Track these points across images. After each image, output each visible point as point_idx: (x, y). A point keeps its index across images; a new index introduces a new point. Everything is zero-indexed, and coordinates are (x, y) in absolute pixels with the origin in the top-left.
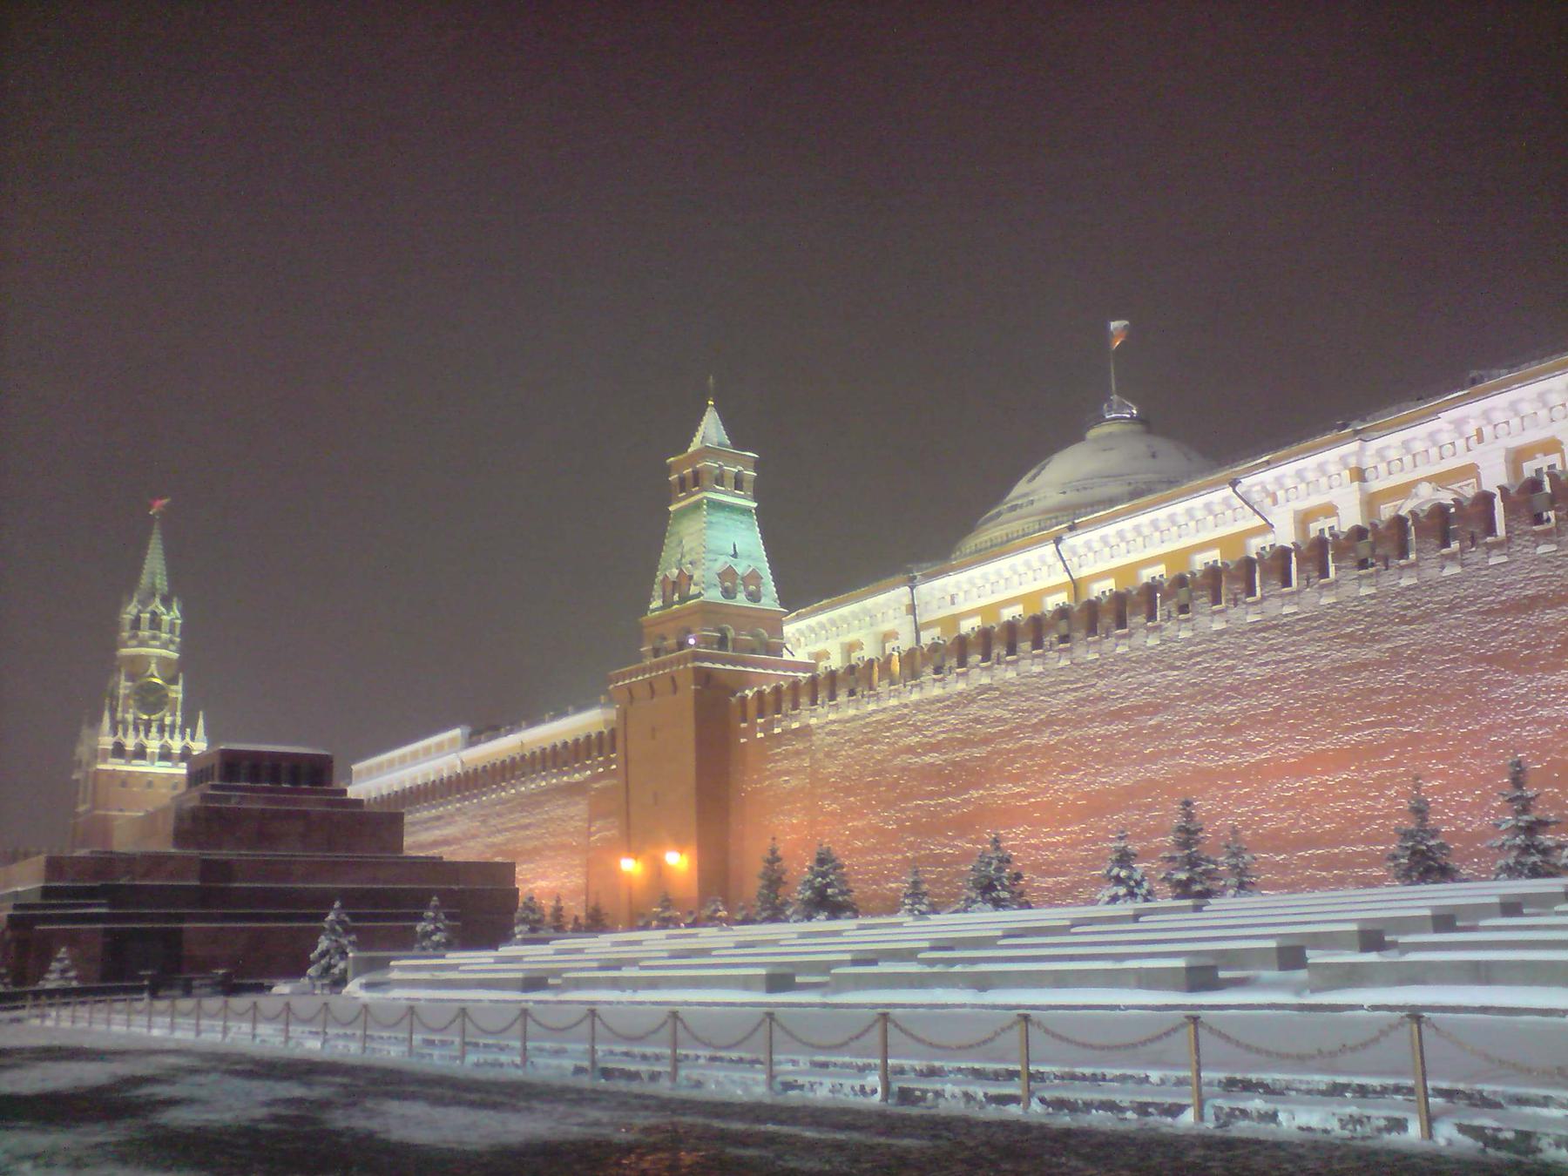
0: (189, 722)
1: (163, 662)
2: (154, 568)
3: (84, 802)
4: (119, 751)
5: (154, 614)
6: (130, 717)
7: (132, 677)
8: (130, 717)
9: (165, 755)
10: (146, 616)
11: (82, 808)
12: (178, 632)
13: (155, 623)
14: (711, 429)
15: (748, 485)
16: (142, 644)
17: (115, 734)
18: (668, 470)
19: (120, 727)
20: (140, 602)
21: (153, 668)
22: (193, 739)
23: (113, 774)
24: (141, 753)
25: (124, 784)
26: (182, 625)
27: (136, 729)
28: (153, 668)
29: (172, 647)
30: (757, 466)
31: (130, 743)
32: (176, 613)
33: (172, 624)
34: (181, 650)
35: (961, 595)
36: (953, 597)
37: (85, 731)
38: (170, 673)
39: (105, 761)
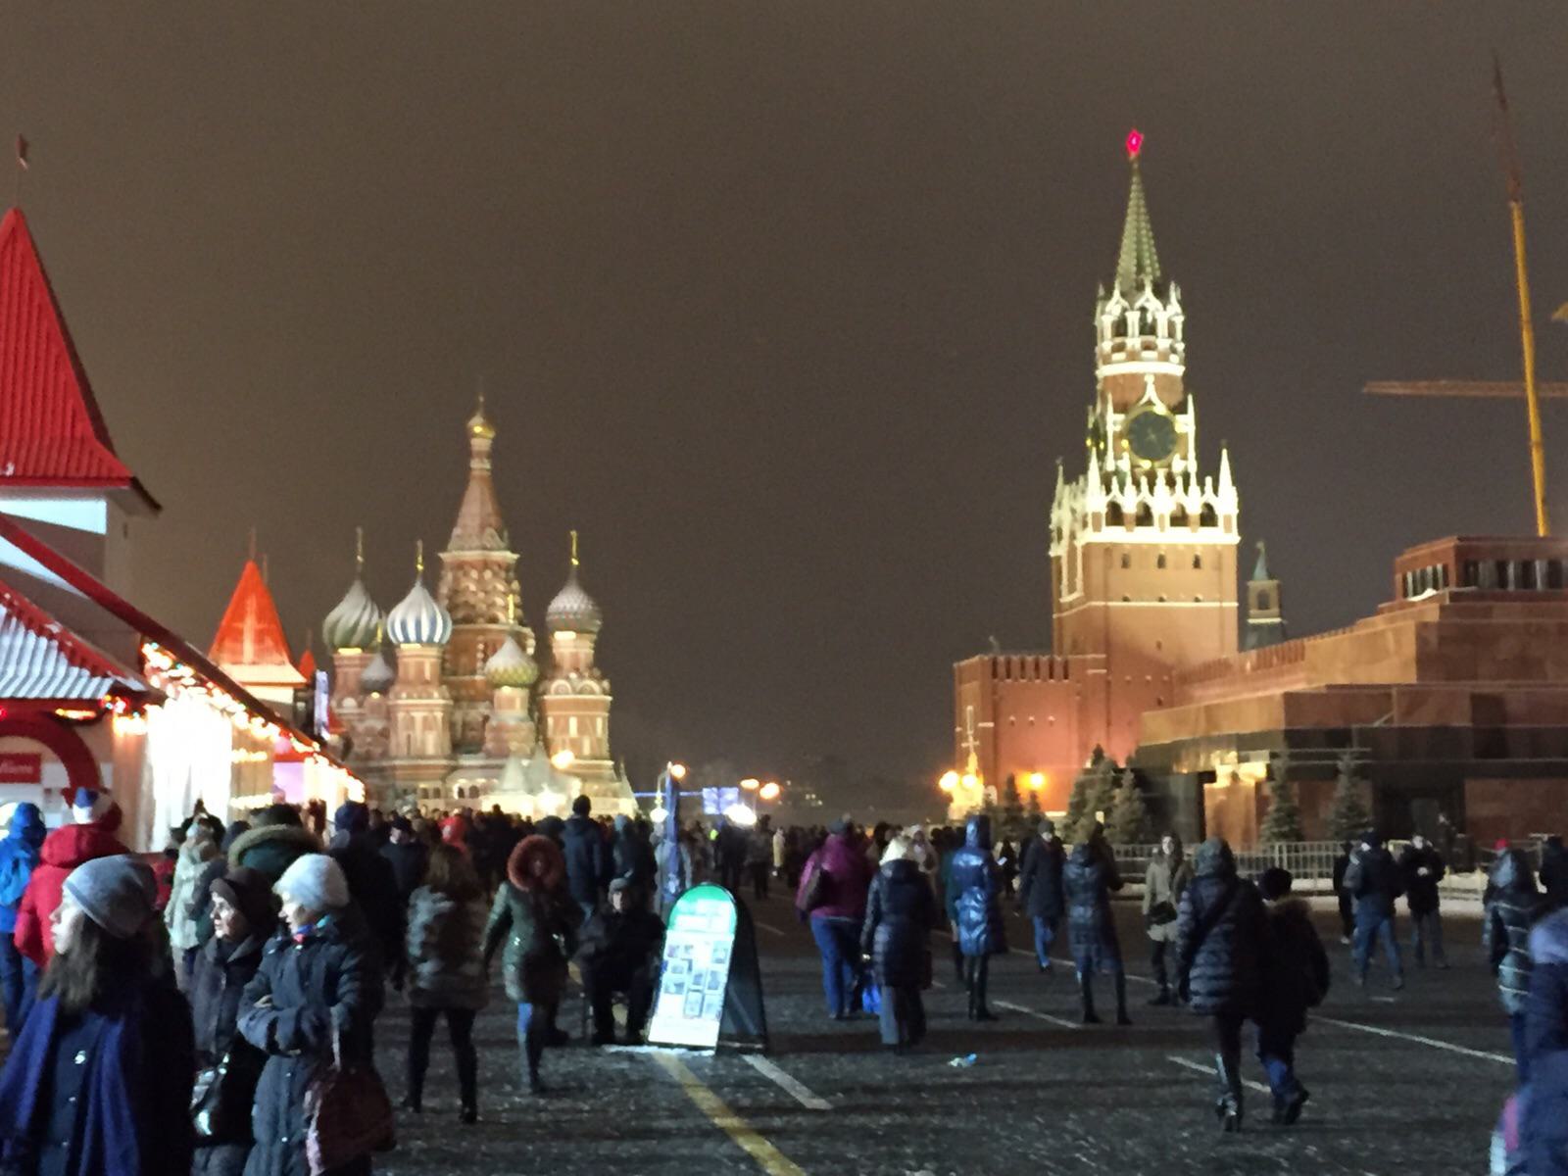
0: (1208, 467)
1: (1163, 381)
3: (1072, 589)
4: (1115, 515)
5: (1143, 310)
6: (1125, 465)
7: (1121, 408)
8: (1125, 465)
9: (1179, 519)
10: (1133, 318)
11: (1067, 598)
12: (1179, 335)
13: (1148, 329)
16: (1133, 357)
17: (1108, 491)
19: (1115, 480)
20: (1123, 295)
21: (1151, 393)
22: (1216, 491)
23: (1108, 550)
24: (1145, 518)
25: (1125, 564)
26: (1185, 324)
27: (1137, 483)
28: (1151, 393)
29: (1174, 358)
31: (1130, 504)
33: (1171, 325)
34: (1189, 360)
37: (1063, 491)
38: (1175, 399)
39: (1097, 528)
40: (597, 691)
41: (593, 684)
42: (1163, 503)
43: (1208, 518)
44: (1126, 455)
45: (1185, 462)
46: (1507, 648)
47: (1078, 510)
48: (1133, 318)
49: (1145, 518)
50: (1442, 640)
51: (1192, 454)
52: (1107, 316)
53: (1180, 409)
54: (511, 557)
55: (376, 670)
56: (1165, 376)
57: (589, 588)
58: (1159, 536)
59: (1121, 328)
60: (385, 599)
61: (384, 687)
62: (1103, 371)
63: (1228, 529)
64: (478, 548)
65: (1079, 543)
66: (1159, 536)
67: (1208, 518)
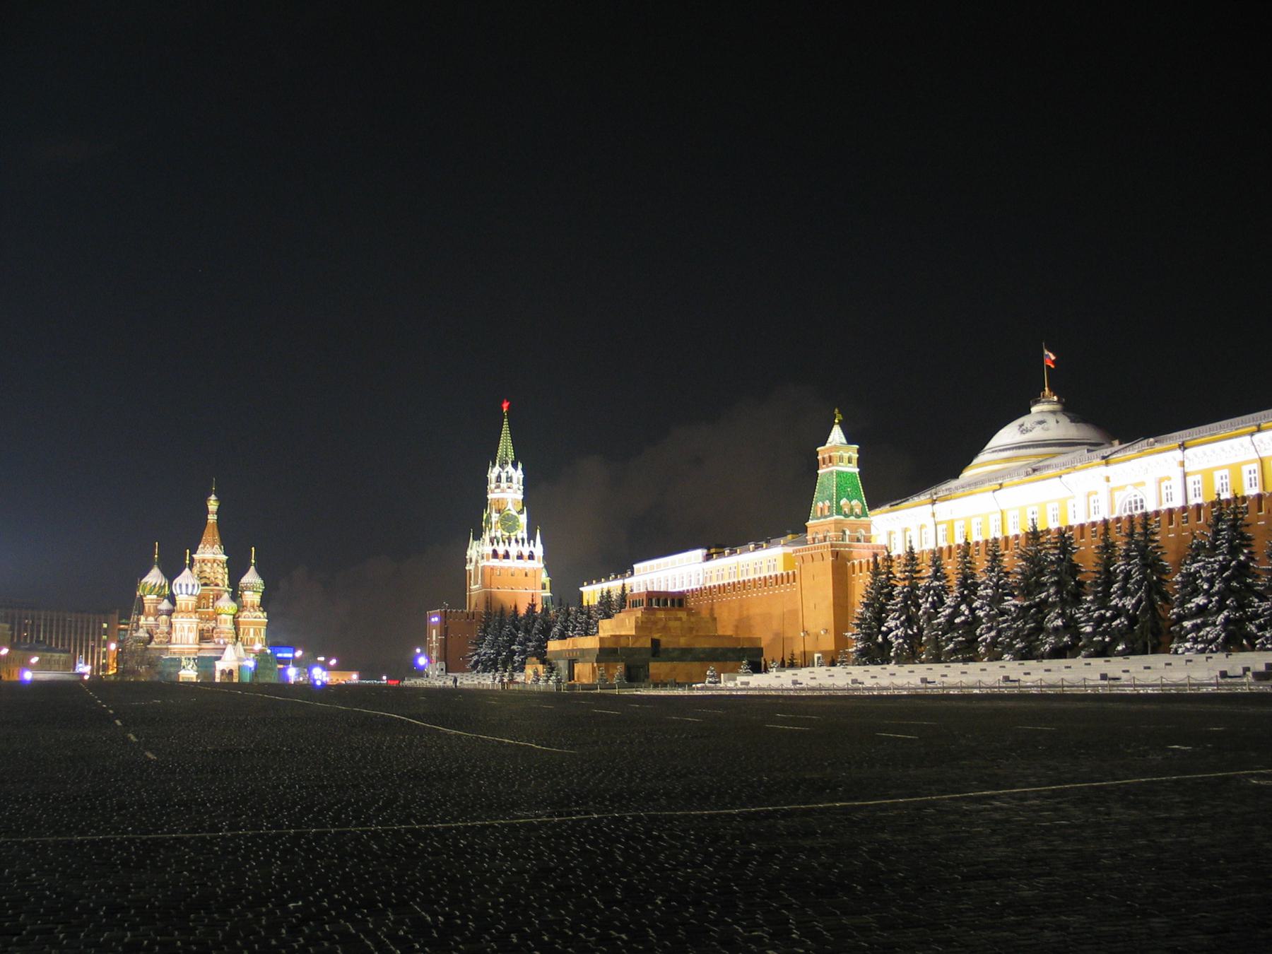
2: (506, 446)
6: (499, 535)
7: (499, 511)
9: (520, 557)
11: (473, 587)
13: (509, 479)
14: (837, 435)
15: (855, 462)
16: (503, 491)
18: (817, 454)
23: (492, 569)
24: (507, 556)
28: (510, 506)
30: (859, 451)
31: (501, 551)
32: (520, 471)
40: (262, 617)
41: (260, 614)
42: (514, 550)
43: (531, 557)
45: (522, 533)
46: (661, 625)
47: (477, 551)
48: (504, 476)
49: (507, 556)
52: (493, 473)
53: (521, 512)
54: (225, 558)
55: (165, 605)
57: (260, 572)
58: (512, 563)
59: (499, 479)
60: (171, 573)
61: (169, 613)
62: (490, 496)
64: (211, 554)
65: (480, 565)
66: (512, 563)
67: (531, 557)
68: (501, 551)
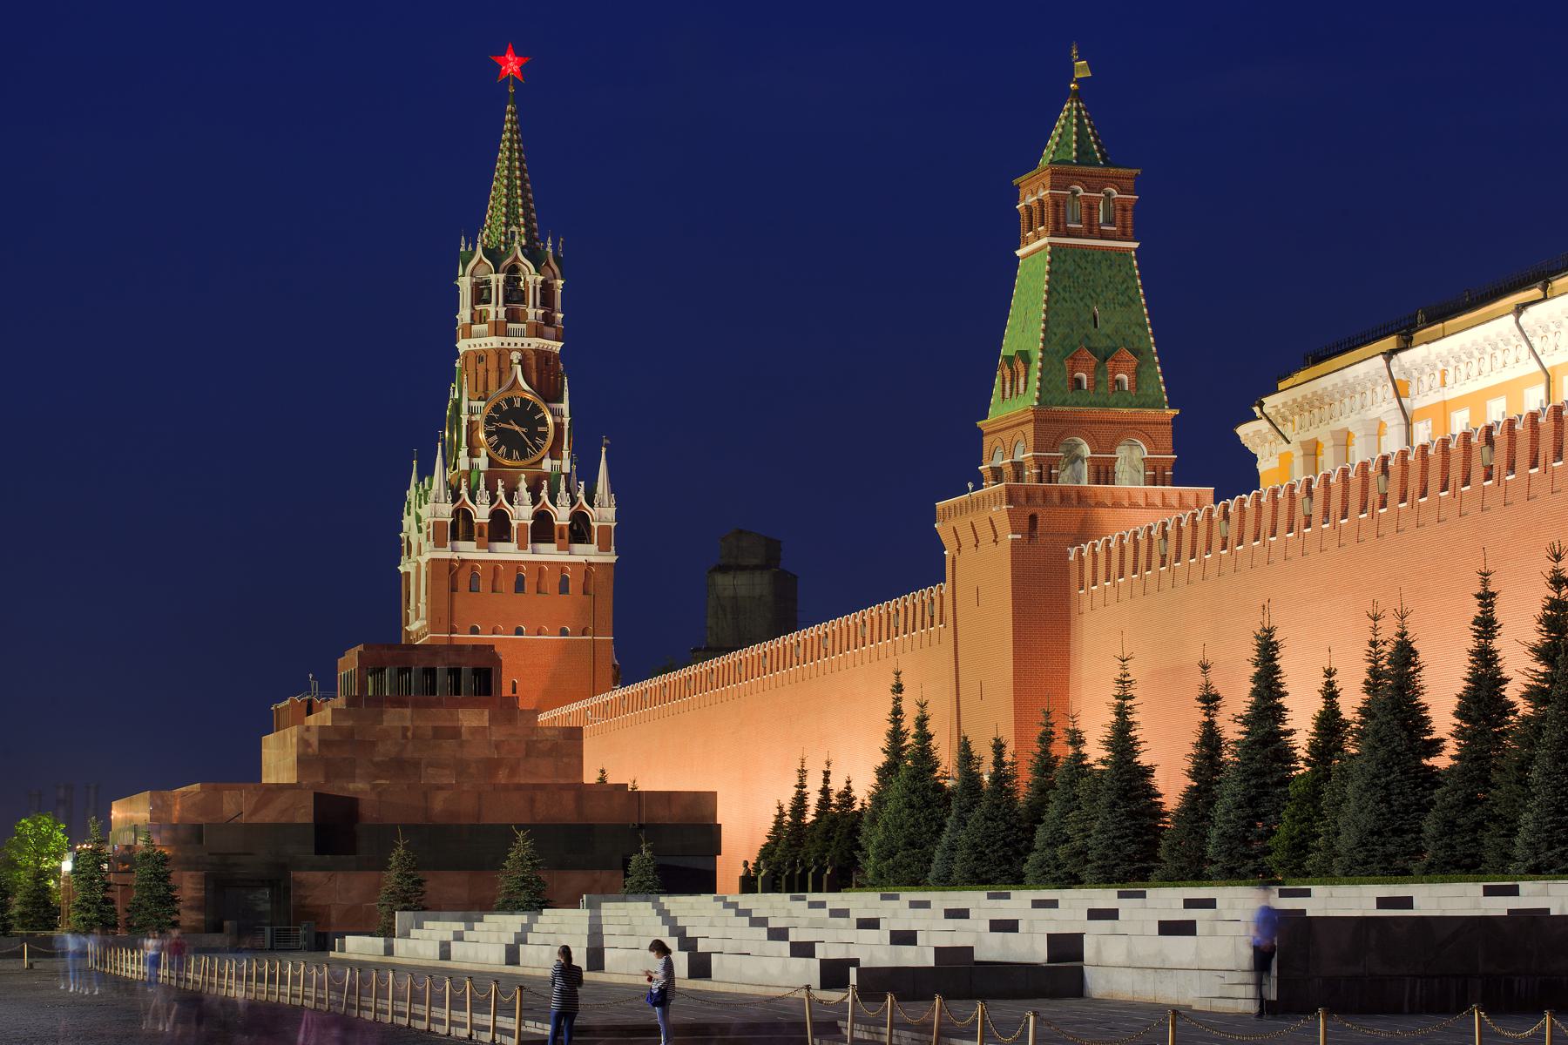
3: (417, 618)
8: (482, 463)
9: (542, 529)
10: (497, 280)
13: (514, 294)
16: (498, 329)
18: (1015, 196)
24: (499, 528)
29: (550, 331)
31: (482, 513)
33: (547, 289)
35: (1451, 370)
36: (1444, 373)
44: (483, 452)
46: (385, 750)
50: (323, 743)
51: (566, 453)
53: (553, 396)
56: (542, 355)
59: (481, 294)
62: (463, 345)
63: (604, 548)
67: (580, 530)
68: (482, 513)
